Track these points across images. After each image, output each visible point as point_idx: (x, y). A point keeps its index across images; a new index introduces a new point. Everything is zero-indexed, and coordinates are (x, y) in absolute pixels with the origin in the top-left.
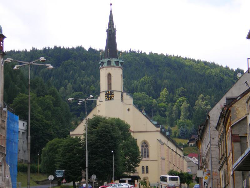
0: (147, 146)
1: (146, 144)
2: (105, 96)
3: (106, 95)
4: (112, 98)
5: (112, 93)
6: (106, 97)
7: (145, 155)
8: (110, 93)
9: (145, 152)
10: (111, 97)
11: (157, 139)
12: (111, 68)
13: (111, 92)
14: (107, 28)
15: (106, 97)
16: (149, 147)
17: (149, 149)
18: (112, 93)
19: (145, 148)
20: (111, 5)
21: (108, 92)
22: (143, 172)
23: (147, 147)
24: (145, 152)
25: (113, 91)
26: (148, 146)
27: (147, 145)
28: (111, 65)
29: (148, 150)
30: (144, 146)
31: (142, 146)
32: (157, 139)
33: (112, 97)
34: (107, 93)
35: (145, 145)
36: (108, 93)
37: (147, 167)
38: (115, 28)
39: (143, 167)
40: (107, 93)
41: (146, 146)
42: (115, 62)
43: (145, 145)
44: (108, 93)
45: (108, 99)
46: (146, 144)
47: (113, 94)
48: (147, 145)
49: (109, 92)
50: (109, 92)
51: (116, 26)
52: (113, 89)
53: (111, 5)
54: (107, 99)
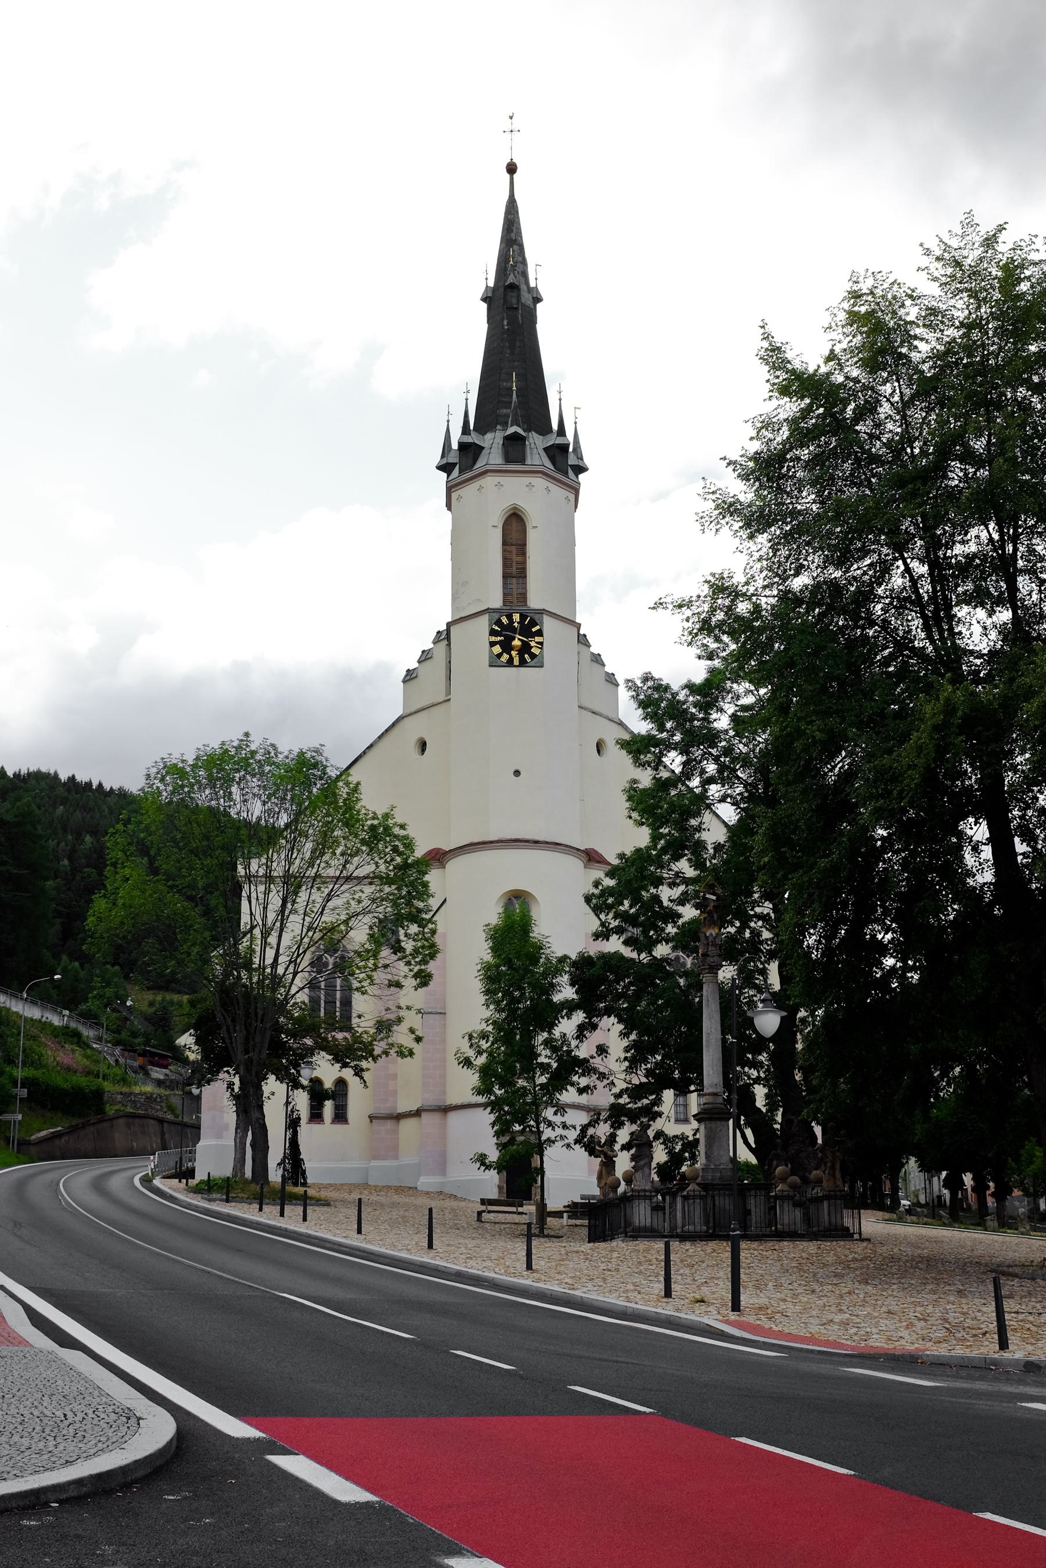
2: (485, 638)
3: (493, 632)
4: (533, 656)
5: (533, 623)
6: (492, 644)
8: (521, 622)
10: (525, 648)
12: (526, 480)
13: (523, 617)
14: (491, 284)
15: (497, 649)
18: (530, 626)
20: (512, 169)
21: (510, 617)
25: (542, 612)
28: (528, 461)
34: (499, 622)
36: (505, 620)
38: (532, 284)
40: (499, 622)
42: (546, 449)
44: (505, 620)
47: (540, 633)
49: (516, 617)
50: (516, 617)
51: (541, 272)
52: (534, 602)
53: (512, 169)
54: (499, 656)
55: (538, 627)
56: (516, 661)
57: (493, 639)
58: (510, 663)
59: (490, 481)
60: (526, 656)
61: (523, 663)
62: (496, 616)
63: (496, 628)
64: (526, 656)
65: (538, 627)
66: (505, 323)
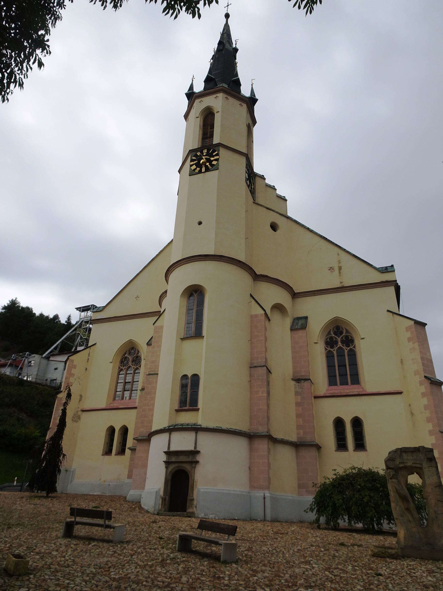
0: (349, 341)
1: (341, 333)
4: (212, 165)
7: (343, 375)
9: (342, 366)
11: (388, 311)
15: (194, 167)
16: (356, 342)
17: (357, 350)
20: (227, 16)
22: (341, 445)
23: (348, 346)
24: (342, 366)
26: (352, 341)
27: (347, 337)
29: (353, 354)
30: (336, 343)
31: (327, 343)
32: (388, 311)
33: (214, 163)
35: (339, 340)
37: (357, 423)
39: (339, 424)
41: (342, 342)
43: (339, 340)
48: (347, 337)
52: (216, 141)
53: (227, 16)
55: (217, 152)
57: (192, 163)
58: (200, 172)
61: (207, 170)
62: (194, 153)
63: (194, 158)
65: (217, 152)
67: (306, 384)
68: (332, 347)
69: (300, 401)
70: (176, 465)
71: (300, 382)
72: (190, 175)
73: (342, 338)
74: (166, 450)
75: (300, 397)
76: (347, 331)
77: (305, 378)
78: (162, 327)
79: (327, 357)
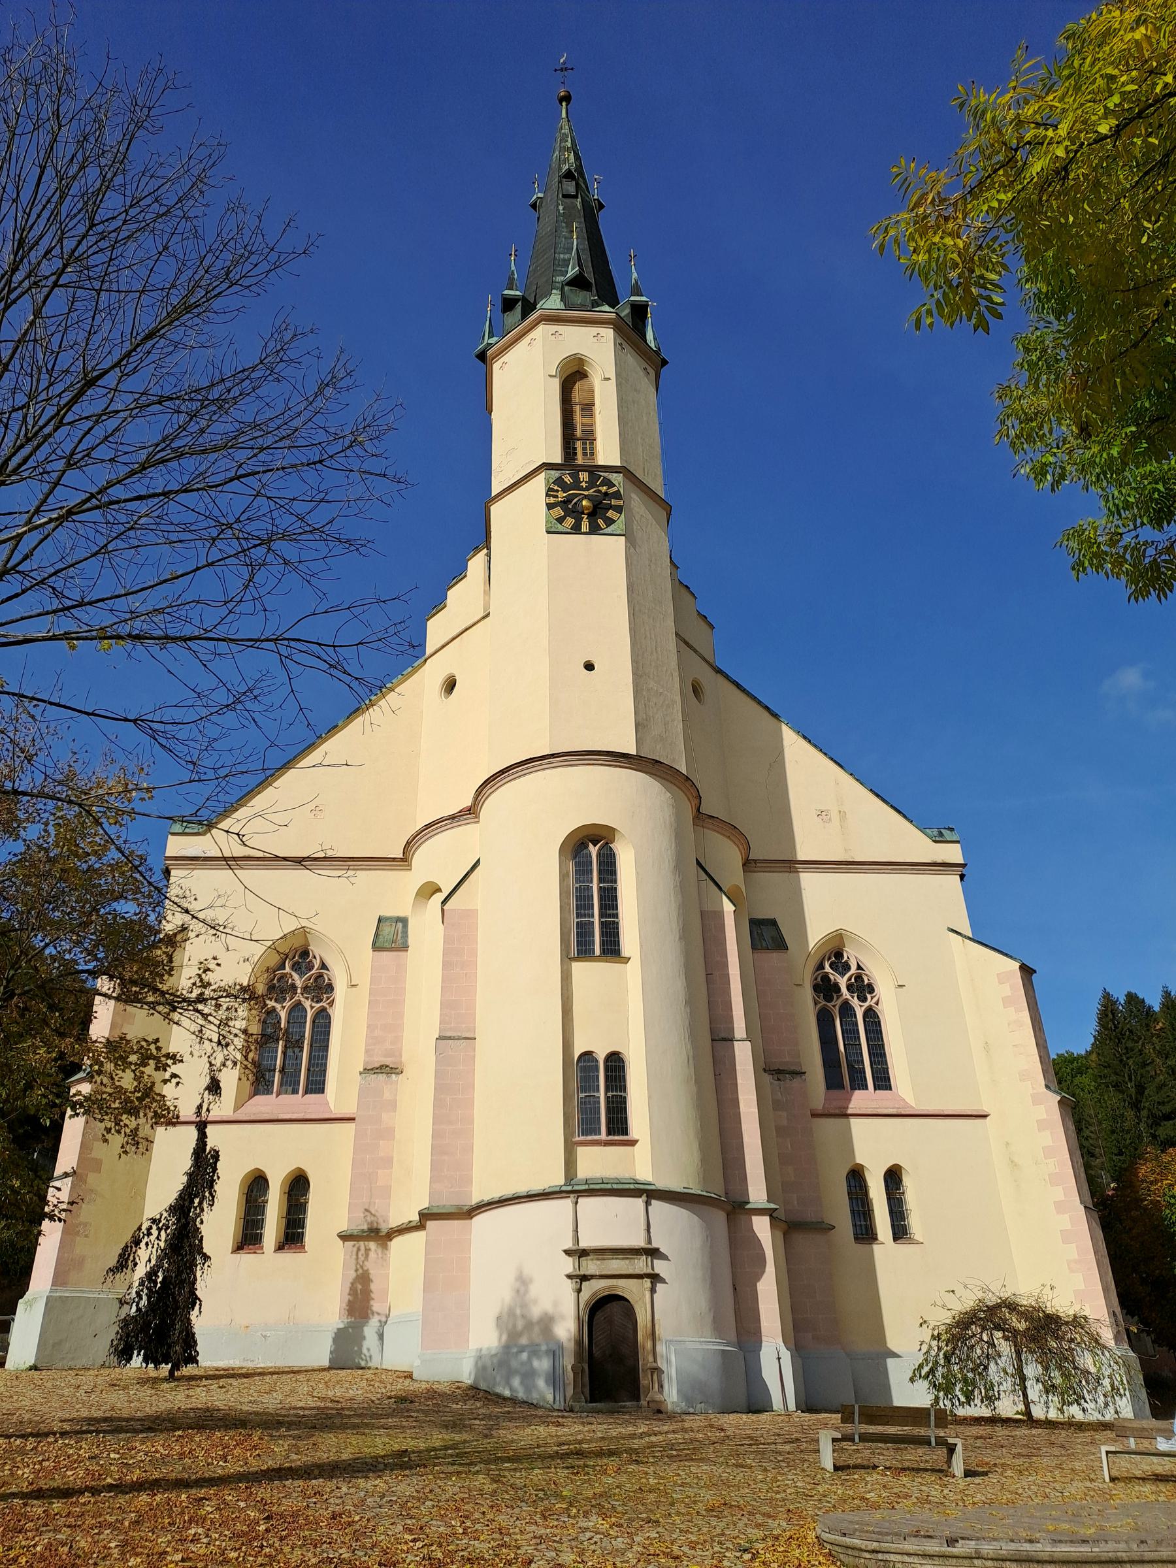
6: (550, 507)
15: (558, 512)
19: (847, 1010)
35: (843, 982)
45: (570, 521)
46: (853, 970)
56: (585, 526)
58: (576, 529)
59: (542, 330)
60: (600, 521)
61: (594, 530)
64: (600, 521)
66: (561, 208)
67: (796, 1082)
68: (829, 998)
69: (785, 1123)
70: (603, 1283)
71: (781, 1076)
72: (548, 532)
73: (849, 979)
74: (569, 1244)
75: (785, 1114)
76: (859, 968)
77: (792, 1068)
78: (471, 914)
79: (818, 1020)
